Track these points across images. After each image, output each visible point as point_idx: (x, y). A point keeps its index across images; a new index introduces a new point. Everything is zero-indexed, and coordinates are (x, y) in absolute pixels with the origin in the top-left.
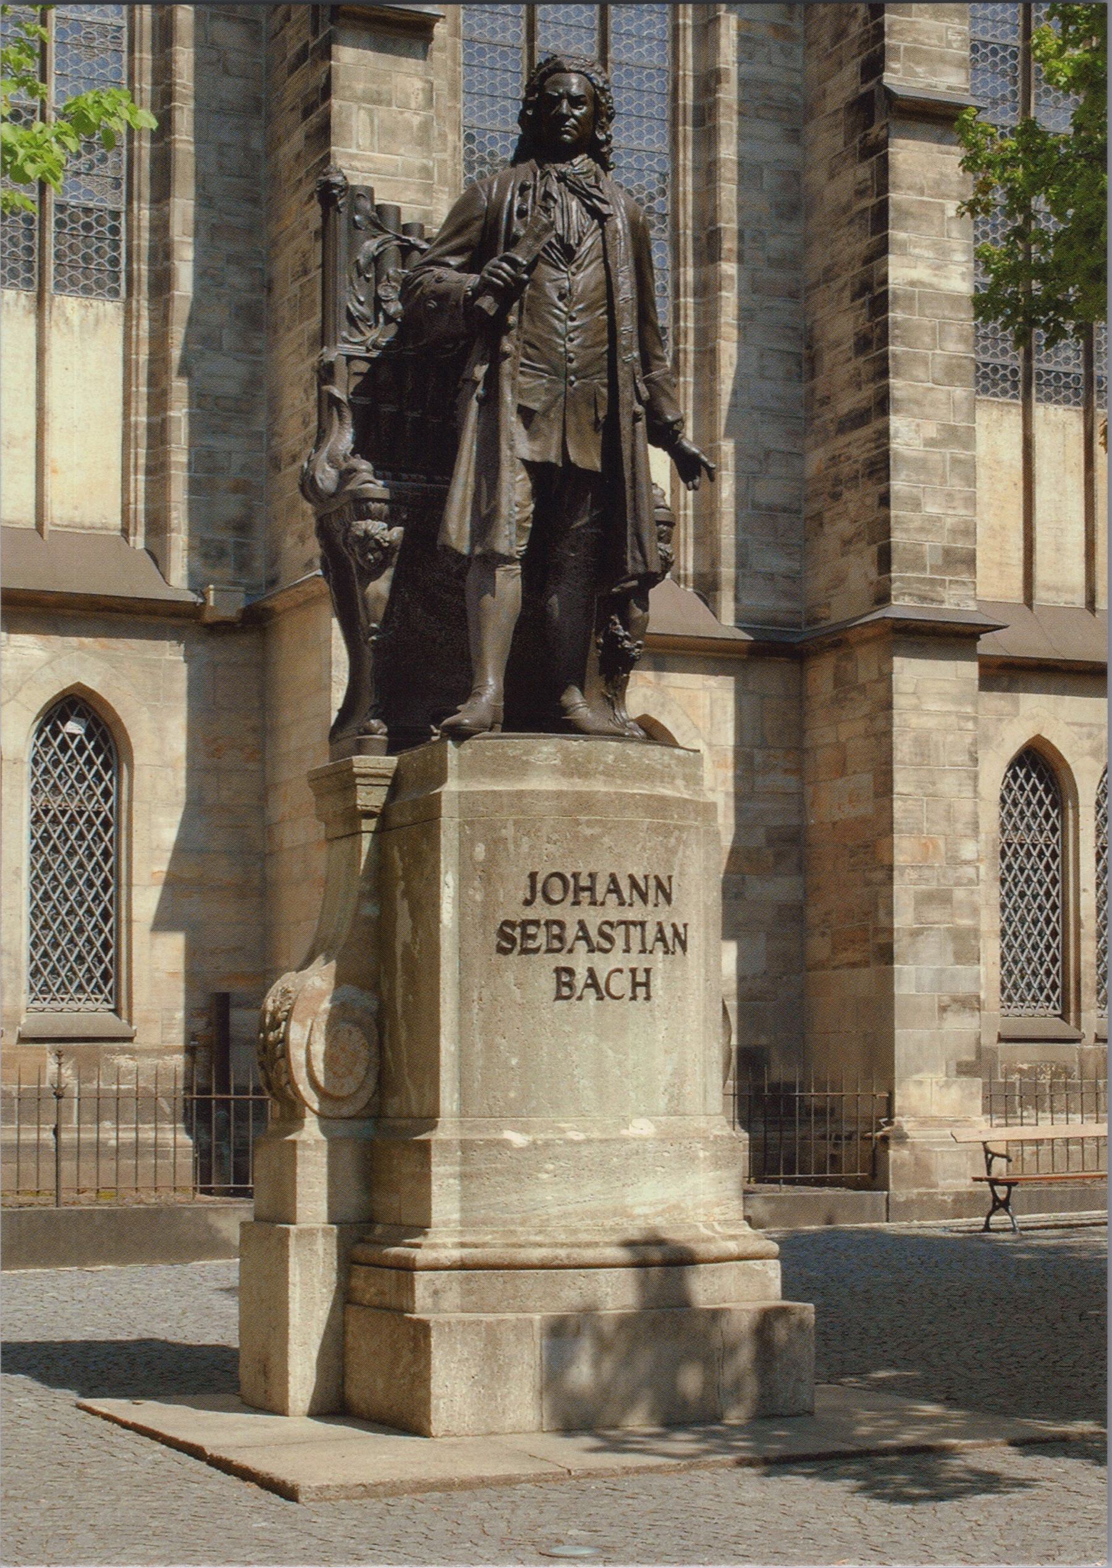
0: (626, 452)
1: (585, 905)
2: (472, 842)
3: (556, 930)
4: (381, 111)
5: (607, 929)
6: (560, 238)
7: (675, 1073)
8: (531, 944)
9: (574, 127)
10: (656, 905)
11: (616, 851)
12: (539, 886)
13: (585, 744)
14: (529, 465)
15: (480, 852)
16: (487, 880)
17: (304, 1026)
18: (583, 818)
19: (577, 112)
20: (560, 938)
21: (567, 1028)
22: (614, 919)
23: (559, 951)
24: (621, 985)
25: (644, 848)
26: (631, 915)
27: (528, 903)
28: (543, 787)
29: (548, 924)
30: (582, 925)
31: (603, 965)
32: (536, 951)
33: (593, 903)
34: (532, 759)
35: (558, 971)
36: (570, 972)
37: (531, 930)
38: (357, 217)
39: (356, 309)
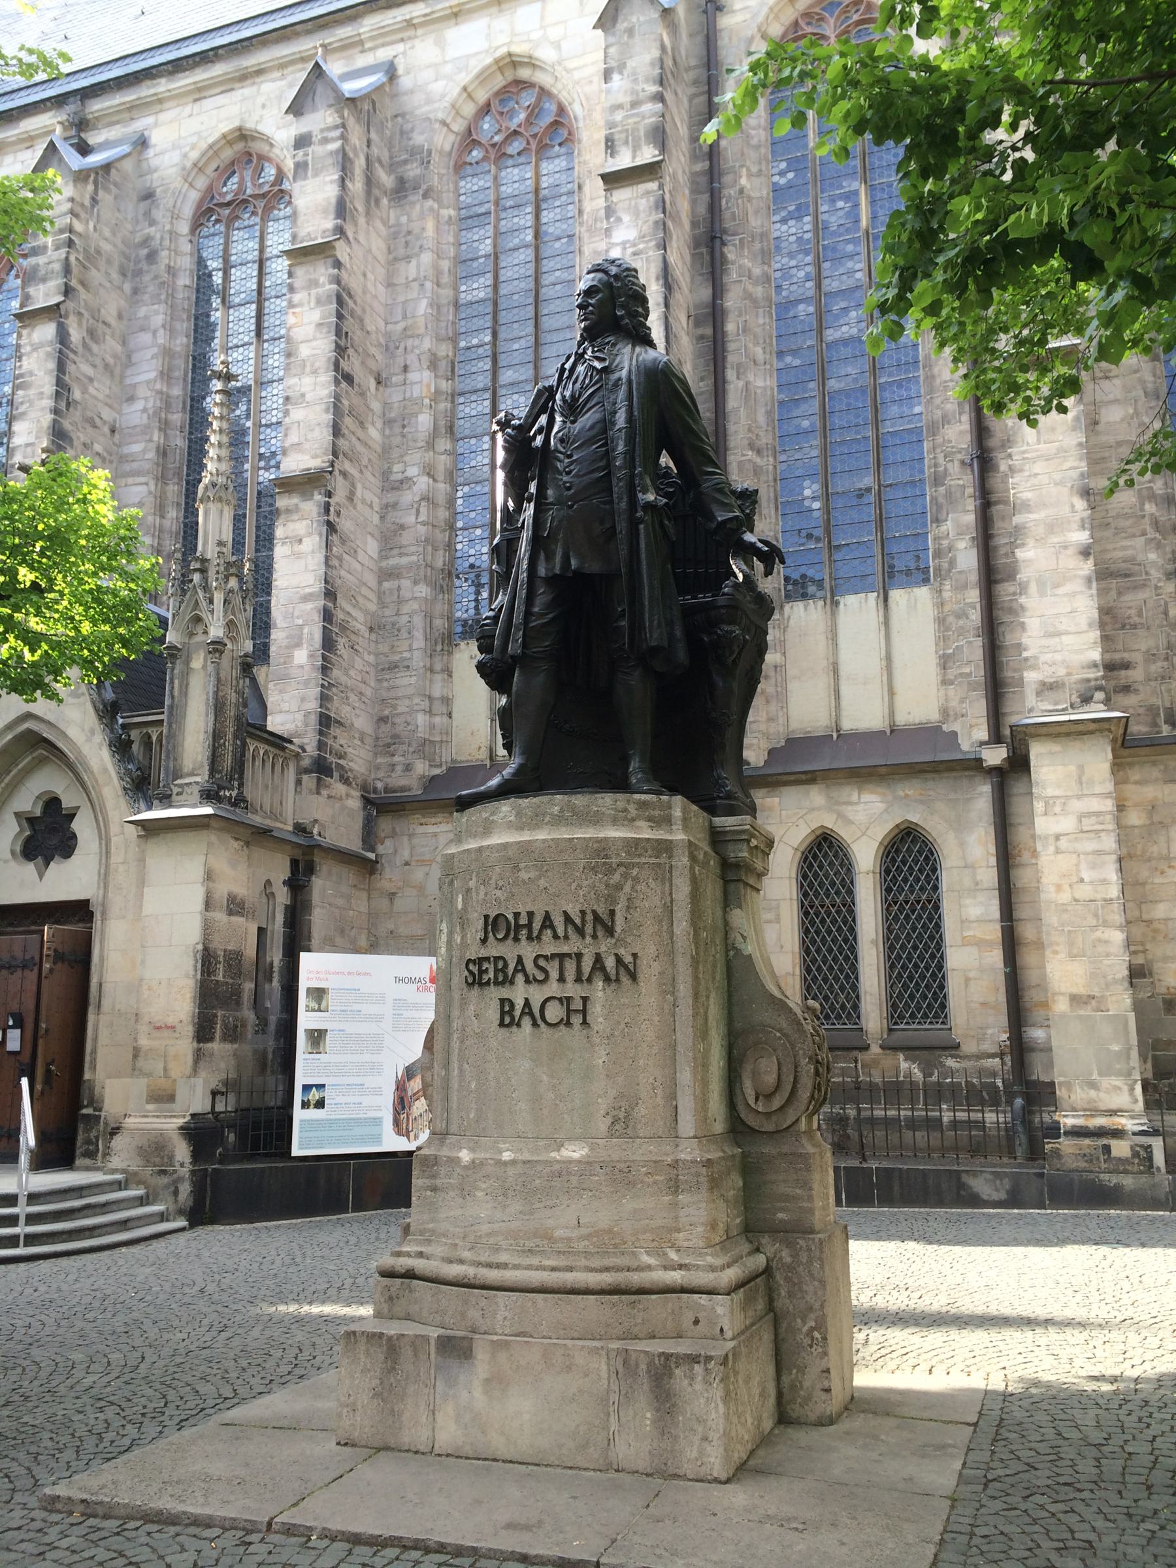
1: (524, 942)
5: (542, 962)
6: (563, 397)
7: (621, 1095)
8: (485, 978)
9: (592, 313)
10: (595, 937)
11: (551, 890)
13: (535, 800)
16: (462, 925)
19: (592, 301)
21: (508, 1054)
22: (548, 951)
23: (502, 983)
24: (554, 1012)
26: (565, 949)
27: (484, 941)
29: (497, 959)
30: (520, 960)
31: (537, 995)
32: (488, 983)
35: (502, 1001)
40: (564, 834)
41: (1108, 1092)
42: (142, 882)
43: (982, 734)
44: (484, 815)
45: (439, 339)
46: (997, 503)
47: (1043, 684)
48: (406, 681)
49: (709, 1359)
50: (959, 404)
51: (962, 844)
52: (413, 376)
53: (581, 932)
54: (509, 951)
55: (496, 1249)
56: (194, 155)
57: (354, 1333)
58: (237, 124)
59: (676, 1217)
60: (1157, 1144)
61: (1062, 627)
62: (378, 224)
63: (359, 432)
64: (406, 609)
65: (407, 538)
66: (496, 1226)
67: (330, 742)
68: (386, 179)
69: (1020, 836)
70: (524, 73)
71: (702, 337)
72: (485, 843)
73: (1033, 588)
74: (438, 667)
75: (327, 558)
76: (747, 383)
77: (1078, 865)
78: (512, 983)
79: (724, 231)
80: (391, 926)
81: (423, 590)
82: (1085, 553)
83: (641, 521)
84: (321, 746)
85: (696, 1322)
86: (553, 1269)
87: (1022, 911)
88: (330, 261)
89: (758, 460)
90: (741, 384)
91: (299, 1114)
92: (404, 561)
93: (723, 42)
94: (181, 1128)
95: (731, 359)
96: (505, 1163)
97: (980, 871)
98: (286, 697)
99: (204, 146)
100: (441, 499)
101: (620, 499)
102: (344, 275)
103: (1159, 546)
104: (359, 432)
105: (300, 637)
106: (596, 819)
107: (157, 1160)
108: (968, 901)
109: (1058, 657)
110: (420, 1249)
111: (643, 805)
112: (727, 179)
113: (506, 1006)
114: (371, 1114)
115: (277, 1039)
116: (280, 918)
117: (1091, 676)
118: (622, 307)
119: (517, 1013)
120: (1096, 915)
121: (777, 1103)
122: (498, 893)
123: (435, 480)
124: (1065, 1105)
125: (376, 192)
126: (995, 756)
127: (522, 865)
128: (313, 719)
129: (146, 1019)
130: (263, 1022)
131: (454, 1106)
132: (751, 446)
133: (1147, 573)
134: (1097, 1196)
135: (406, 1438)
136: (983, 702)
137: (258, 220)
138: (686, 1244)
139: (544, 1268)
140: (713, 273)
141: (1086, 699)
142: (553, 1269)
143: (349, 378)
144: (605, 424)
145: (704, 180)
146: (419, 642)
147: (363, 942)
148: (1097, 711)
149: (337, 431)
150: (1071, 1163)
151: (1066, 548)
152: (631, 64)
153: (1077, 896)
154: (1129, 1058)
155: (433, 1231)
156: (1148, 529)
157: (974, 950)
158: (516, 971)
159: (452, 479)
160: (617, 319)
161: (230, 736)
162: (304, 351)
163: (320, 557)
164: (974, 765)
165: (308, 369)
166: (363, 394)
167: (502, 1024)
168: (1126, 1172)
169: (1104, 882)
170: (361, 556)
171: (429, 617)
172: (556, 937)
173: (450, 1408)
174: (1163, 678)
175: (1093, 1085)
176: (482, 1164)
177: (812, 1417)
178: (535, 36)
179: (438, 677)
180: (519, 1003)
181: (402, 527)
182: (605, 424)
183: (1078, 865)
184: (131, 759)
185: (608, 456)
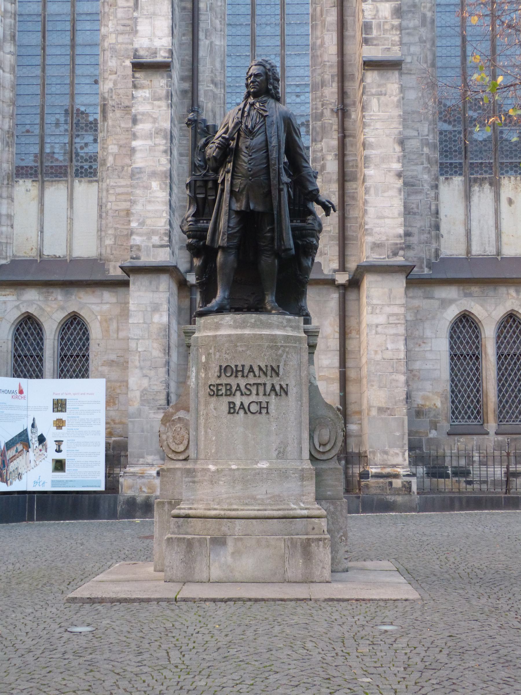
0: (275, 204)
2: (201, 355)
3: (228, 387)
4: (382, 98)
5: (248, 387)
7: (282, 442)
8: (220, 393)
9: (257, 85)
10: (271, 377)
12: (223, 371)
13: (243, 316)
14: (237, 213)
15: (203, 359)
16: (206, 370)
17: (166, 426)
18: (238, 344)
19: (258, 80)
20: (230, 390)
21: (232, 425)
22: (252, 382)
23: (230, 395)
24: (254, 408)
25: (265, 355)
26: (259, 381)
27: (219, 377)
28: (226, 333)
29: (226, 385)
30: (238, 385)
32: (222, 395)
33: (243, 376)
34: (222, 322)
35: (229, 403)
37: (220, 388)
38: (199, 131)
39: (197, 163)
40: (258, 332)
41: (392, 456)
43: (335, 265)
44: (216, 320)
46: (349, 136)
47: (374, 244)
49: (325, 539)
50: (332, 76)
53: (265, 374)
54: (233, 382)
55: (232, 504)
57: (172, 538)
60: (414, 481)
61: (386, 214)
66: (231, 495)
69: (351, 322)
71: (184, 9)
72: (219, 333)
73: (372, 191)
76: (211, 43)
77: (385, 341)
78: (234, 395)
82: (399, 175)
85: (313, 529)
86: (258, 510)
87: (350, 363)
89: (215, 90)
90: (207, 42)
95: (202, 25)
96: (234, 470)
97: (330, 340)
101: (274, 179)
103: (429, 172)
106: (269, 326)
108: (323, 357)
109: (383, 230)
111: (289, 321)
117: (398, 242)
118: (271, 84)
119: (237, 408)
120: (393, 367)
121: (328, 448)
122: (227, 356)
123: (4, 71)
124: (372, 463)
126: (342, 279)
127: (238, 344)
131: (202, 447)
132: (213, 82)
133: (422, 186)
134: (386, 507)
135: (197, 577)
136: (337, 248)
139: (254, 510)
141: (395, 254)
142: (258, 510)
148: (399, 260)
150: (373, 491)
151: (390, 171)
153: (385, 357)
154: (403, 439)
155: (193, 500)
156: (425, 160)
158: (236, 390)
159: (14, 72)
164: (331, 282)
167: (229, 413)
168: (399, 494)
169: (398, 350)
172: (255, 376)
173: (217, 564)
174: (427, 243)
175: (386, 453)
176: (222, 470)
177: (340, 569)
179: (5, 201)
182: (267, 142)
183: (385, 341)
185: (268, 157)
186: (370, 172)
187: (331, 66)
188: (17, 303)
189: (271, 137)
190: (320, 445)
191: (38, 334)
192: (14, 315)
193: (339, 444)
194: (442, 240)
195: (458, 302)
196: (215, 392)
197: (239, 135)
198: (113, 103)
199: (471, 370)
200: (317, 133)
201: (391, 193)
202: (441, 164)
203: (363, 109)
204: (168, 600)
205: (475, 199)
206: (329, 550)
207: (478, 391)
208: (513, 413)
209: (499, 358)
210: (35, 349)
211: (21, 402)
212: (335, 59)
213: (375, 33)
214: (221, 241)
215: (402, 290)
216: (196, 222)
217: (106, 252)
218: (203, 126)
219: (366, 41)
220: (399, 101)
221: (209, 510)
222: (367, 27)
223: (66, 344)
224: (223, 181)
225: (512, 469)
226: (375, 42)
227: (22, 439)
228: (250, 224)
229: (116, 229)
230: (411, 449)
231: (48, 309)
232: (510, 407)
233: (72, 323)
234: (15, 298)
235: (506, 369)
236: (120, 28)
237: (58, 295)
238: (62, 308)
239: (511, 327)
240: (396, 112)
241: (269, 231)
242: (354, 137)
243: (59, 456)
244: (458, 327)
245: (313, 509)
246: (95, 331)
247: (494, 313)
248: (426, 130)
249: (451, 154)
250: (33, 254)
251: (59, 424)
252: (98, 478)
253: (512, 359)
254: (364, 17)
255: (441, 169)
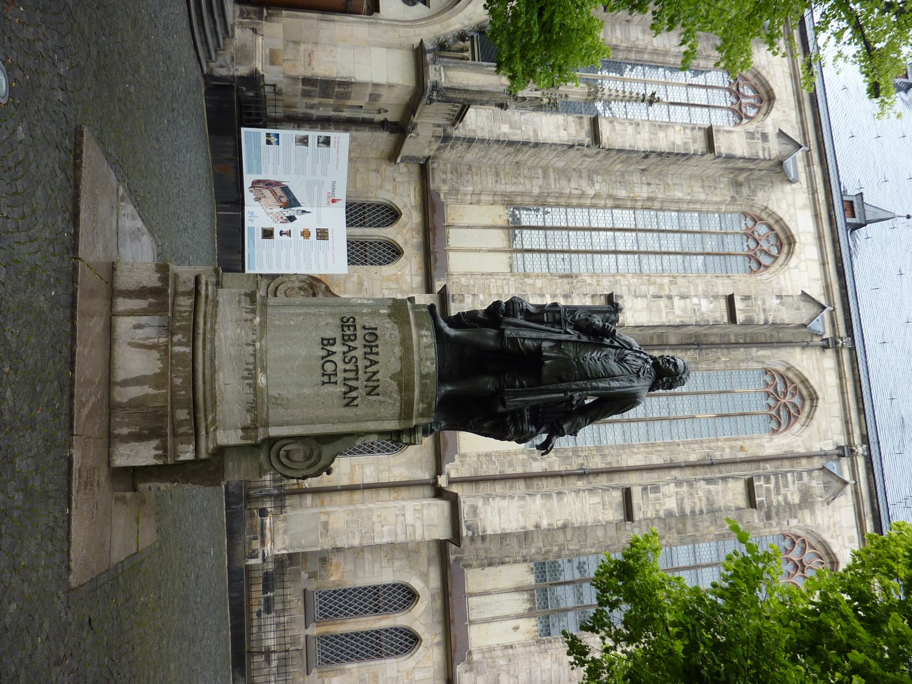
0: (551, 387)
1: (364, 350)
3: (352, 338)
5: (354, 360)
6: (626, 355)
10: (366, 386)
14: (540, 347)
16: (371, 313)
22: (360, 364)
23: (343, 339)
24: (329, 367)
26: (360, 372)
27: (364, 328)
29: (355, 335)
30: (355, 348)
32: (343, 330)
33: (365, 353)
35: (334, 339)
36: (334, 344)
42: (389, 47)
43: (453, 475)
44: (426, 324)
45: (662, 202)
48: (490, 181)
51: (400, 465)
52: (645, 188)
53: (368, 380)
54: (359, 343)
56: (764, 73)
58: (777, 97)
59: (230, 429)
60: (258, 561)
62: (721, 173)
63: (619, 161)
64: (527, 182)
65: (564, 182)
67: (459, 142)
68: (741, 178)
69: (404, 493)
70: (785, 249)
71: (652, 339)
73: (522, 503)
74: (496, 198)
75: (555, 144)
78: (344, 344)
79: (701, 349)
80: (362, 170)
81: (536, 191)
82: (537, 526)
83: (566, 394)
84: (458, 138)
87: (367, 493)
88: (705, 150)
91: (263, 131)
92: (552, 181)
93: (789, 350)
94: (256, 70)
96: (254, 345)
98: (484, 119)
99: (768, 78)
100: (582, 201)
102: (697, 157)
103: (538, 553)
104: (619, 161)
105: (515, 128)
107: (239, 56)
109: (489, 514)
110: (210, 297)
112: (725, 351)
113: (332, 341)
114: (263, 168)
115: (303, 113)
116: (367, 116)
118: (667, 381)
119: (329, 348)
121: (284, 460)
125: (737, 172)
126: (442, 481)
128: (472, 135)
129: (315, 49)
130: (312, 107)
131: (281, 311)
137: (729, 105)
138: (218, 434)
139: (204, 369)
140: (682, 344)
141: (468, 528)
143: (646, 157)
144: (611, 376)
145: (725, 340)
146: (509, 189)
147: (353, 155)
148: (464, 532)
149: (620, 151)
152: (783, 309)
157: (349, 471)
158: (349, 346)
160: (661, 378)
161: (465, 96)
162: (661, 135)
163: (556, 141)
164: (439, 471)
165: (653, 136)
166: (638, 163)
167: (323, 339)
170: (556, 159)
171: (522, 194)
172: (366, 367)
175: (285, 532)
178: (802, 256)
180: (333, 349)
181: (569, 180)
184: (455, 41)
185: (598, 377)
186: (538, 500)
187: (618, 461)
188: (408, 205)
189: (617, 380)
190: (288, 452)
191: (384, 223)
192: (399, 203)
193: (288, 473)
194: (479, 570)
195: (426, 589)
196: (347, 323)
197: (616, 348)
198: (575, 283)
199: (365, 607)
200: (562, 453)
201: (521, 519)
202: (544, 564)
203: (591, 491)
204: (75, 248)
205: (516, 596)
206: (152, 462)
207: (346, 615)
208: (326, 650)
209: (377, 632)
210: (370, 220)
211: (324, 200)
212: (624, 464)
213: (652, 496)
214: (509, 332)
215: (437, 537)
216: (522, 311)
217: (454, 279)
218: (613, 317)
219: (645, 489)
220: (599, 521)
221: (205, 317)
222: (656, 489)
223: (375, 246)
224: (569, 333)
225: (274, 656)
226: (645, 497)
227: (292, 202)
228: (527, 363)
229: (474, 286)
230: (290, 556)
231: (405, 231)
232: (332, 647)
233: (393, 251)
234: (413, 204)
235: (368, 639)
236: (633, 288)
237: (417, 239)
238: (406, 243)
239: (406, 640)
240: (590, 520)
241: (520, 383)
242: (562, 484)
243: (276, 234)
244: (404, 591)
245: (207, 442)
246: (387, 270)
247: (418, 623)
248: (573, 547)
249: (554, 571)
250: (450, 221)
251: (306, 234)
252: (257, 268)
253: (377, 644)
254: (664, 485)
255: (540, 564)
